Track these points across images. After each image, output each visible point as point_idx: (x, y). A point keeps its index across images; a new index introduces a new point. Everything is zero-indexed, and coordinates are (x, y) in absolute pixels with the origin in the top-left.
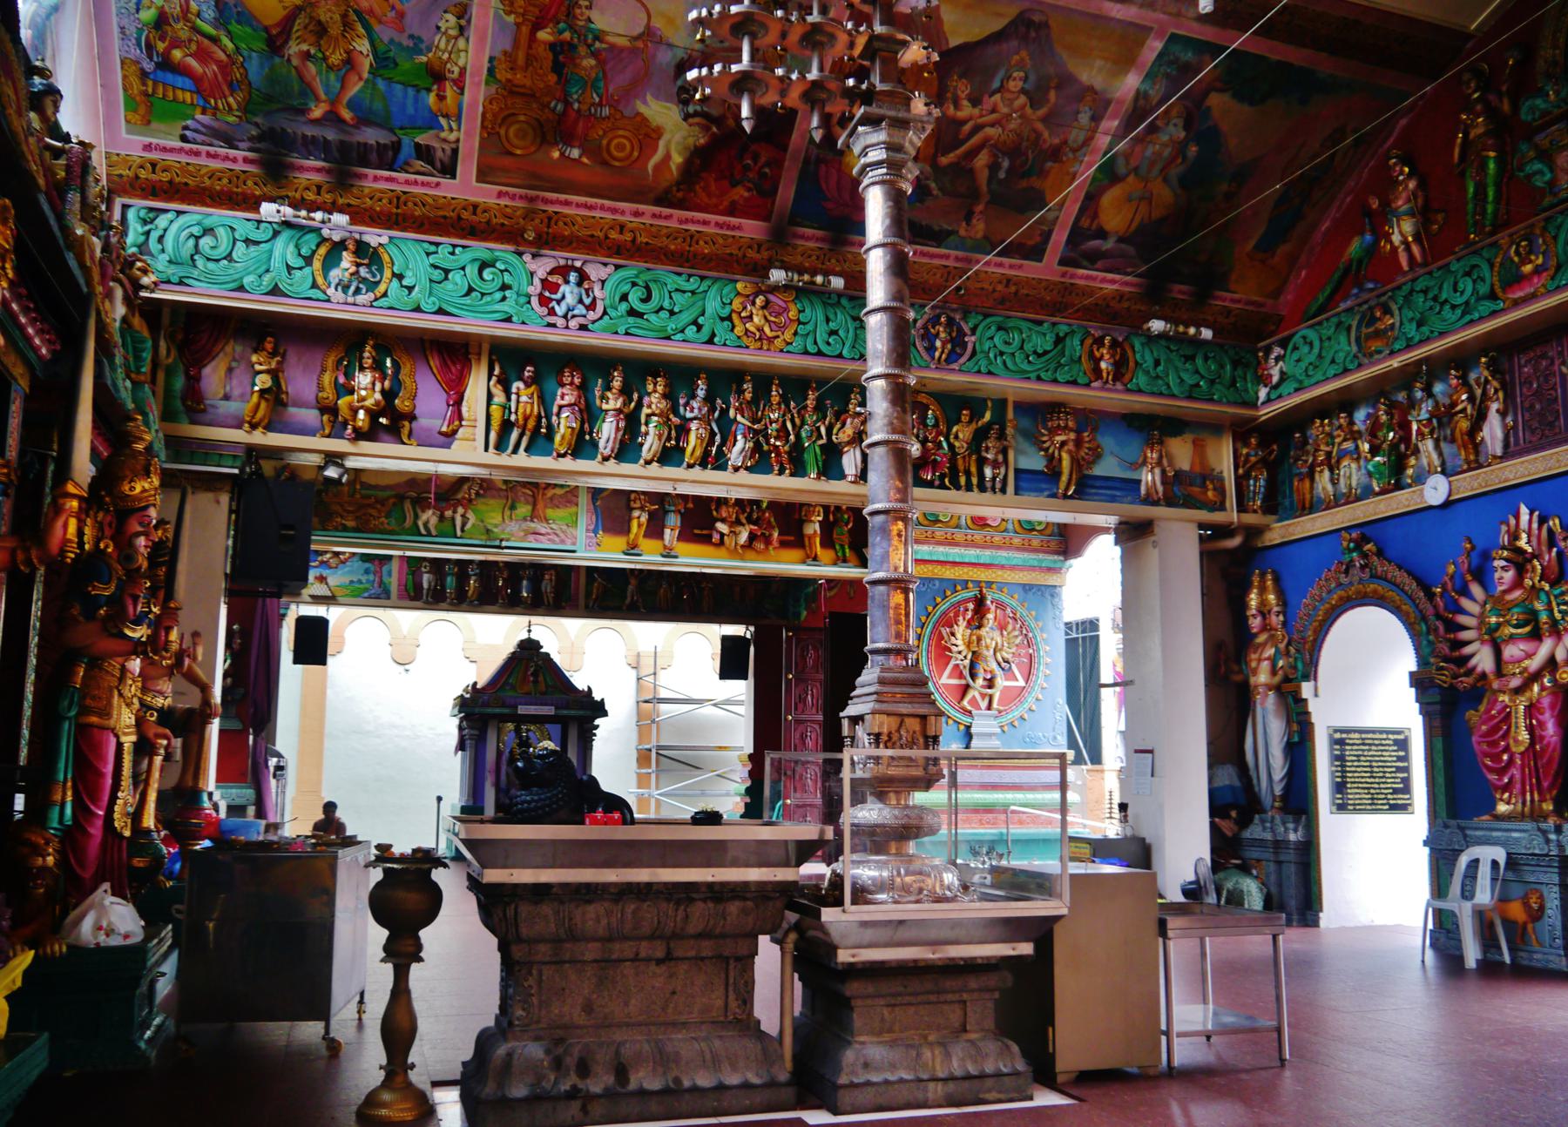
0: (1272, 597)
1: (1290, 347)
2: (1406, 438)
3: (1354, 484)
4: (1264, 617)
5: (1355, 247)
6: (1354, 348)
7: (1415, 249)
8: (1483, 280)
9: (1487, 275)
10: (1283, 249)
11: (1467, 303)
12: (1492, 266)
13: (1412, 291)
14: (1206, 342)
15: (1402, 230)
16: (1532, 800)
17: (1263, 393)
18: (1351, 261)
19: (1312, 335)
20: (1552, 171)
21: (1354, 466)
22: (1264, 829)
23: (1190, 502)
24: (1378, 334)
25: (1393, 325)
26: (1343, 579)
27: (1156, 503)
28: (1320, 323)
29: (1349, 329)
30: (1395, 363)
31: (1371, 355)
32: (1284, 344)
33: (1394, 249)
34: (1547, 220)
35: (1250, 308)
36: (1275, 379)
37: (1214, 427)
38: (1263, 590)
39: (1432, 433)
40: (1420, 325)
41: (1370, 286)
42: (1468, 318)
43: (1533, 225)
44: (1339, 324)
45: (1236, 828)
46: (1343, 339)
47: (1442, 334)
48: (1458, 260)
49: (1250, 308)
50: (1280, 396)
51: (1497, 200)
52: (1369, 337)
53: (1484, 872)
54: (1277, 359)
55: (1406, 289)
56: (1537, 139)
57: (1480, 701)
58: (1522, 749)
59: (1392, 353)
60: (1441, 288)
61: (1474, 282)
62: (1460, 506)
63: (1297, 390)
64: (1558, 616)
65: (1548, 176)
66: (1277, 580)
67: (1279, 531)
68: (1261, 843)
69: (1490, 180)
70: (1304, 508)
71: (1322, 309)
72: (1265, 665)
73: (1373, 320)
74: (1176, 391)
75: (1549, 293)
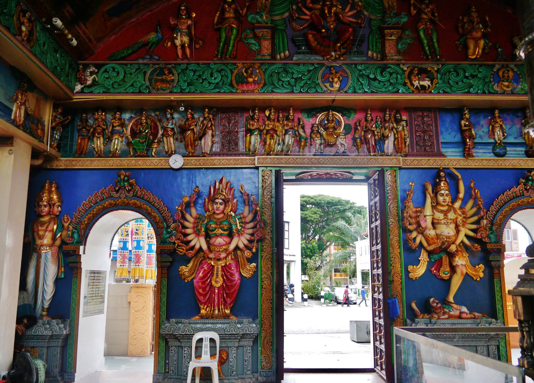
0: (55, 197)
1: (102, 70)
2: (155, 135)
3: (119, 148)
4: (50, 208)
5: (152, 37)
6: (148, 83)
7: (188, 51)
8: (227, 77)
9: (230, 76)
10: (116, 19)
11: (217, 84)
12: (232, 73)
13: (187, 68)
14: (71, 46)
15: (181, 39)
16: (222, 309)
17: (78, 87)
18: (148, 42)
19: (118, 68)
20: (260, 46)
21: (120, 139)
22: (45, 329)
23: (31, 134)
24: (162, 81)
25: (173, 81)
26: (114, 194)
27: (18, 127)
28: (126, 64)
29: (145, 73)
30: (172, 97)
31: (158, 89)
32: (99, 67)
33: (174, 45)
34: (261, 64)
35: (87, 40)
36: (89, 83)
37: (44, 95)
38: (50, 192)
39: (174, 135)
40: (189, 85)
41: (157, 57)
42: (217, 90)
43: (254, 64)
44: (139, 68)
45: (24, 329)
46: (141, 77)
47: (201, 93)
48: (215, 64)
49: (87, 40)
50: (92, 92)
51: (233, 46)
52: (157, 81)
53: (206, 344)
54: (92, 73)
55: (183, 67)
56: (257, 31)
57: (189, 263)
58: (219, 285)
59: (171, 93)
60: (203, 72)
61: (222, 76)
62: (184, 171)
63: (104, 92)
64: (239, 228)
65: (257, 48)
66: (57, 188)
67: (63, 163)
68: (42, 337)
69: (233, 37)
70: (71, 152)
71: (123, 59)
72: (49, 235)
73: (162, 73)
74: (49, 65)
75: (260, 93)
